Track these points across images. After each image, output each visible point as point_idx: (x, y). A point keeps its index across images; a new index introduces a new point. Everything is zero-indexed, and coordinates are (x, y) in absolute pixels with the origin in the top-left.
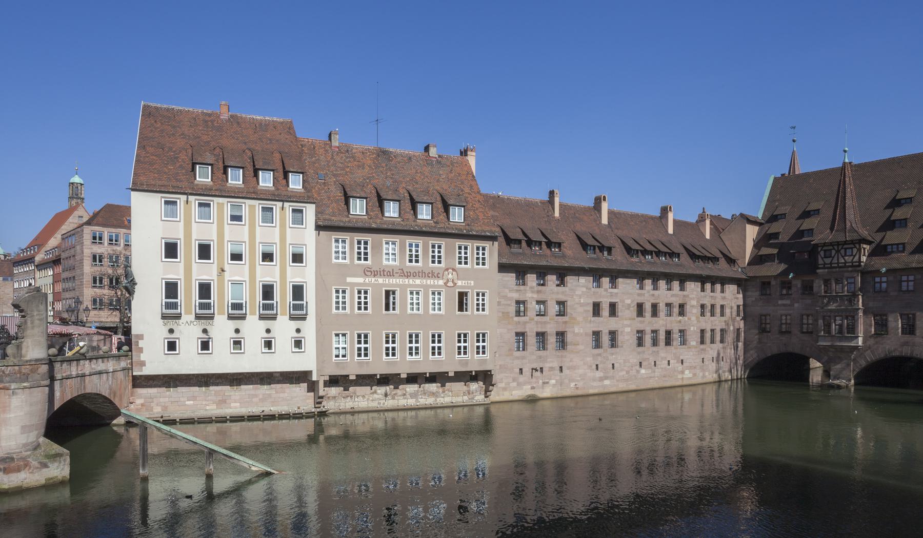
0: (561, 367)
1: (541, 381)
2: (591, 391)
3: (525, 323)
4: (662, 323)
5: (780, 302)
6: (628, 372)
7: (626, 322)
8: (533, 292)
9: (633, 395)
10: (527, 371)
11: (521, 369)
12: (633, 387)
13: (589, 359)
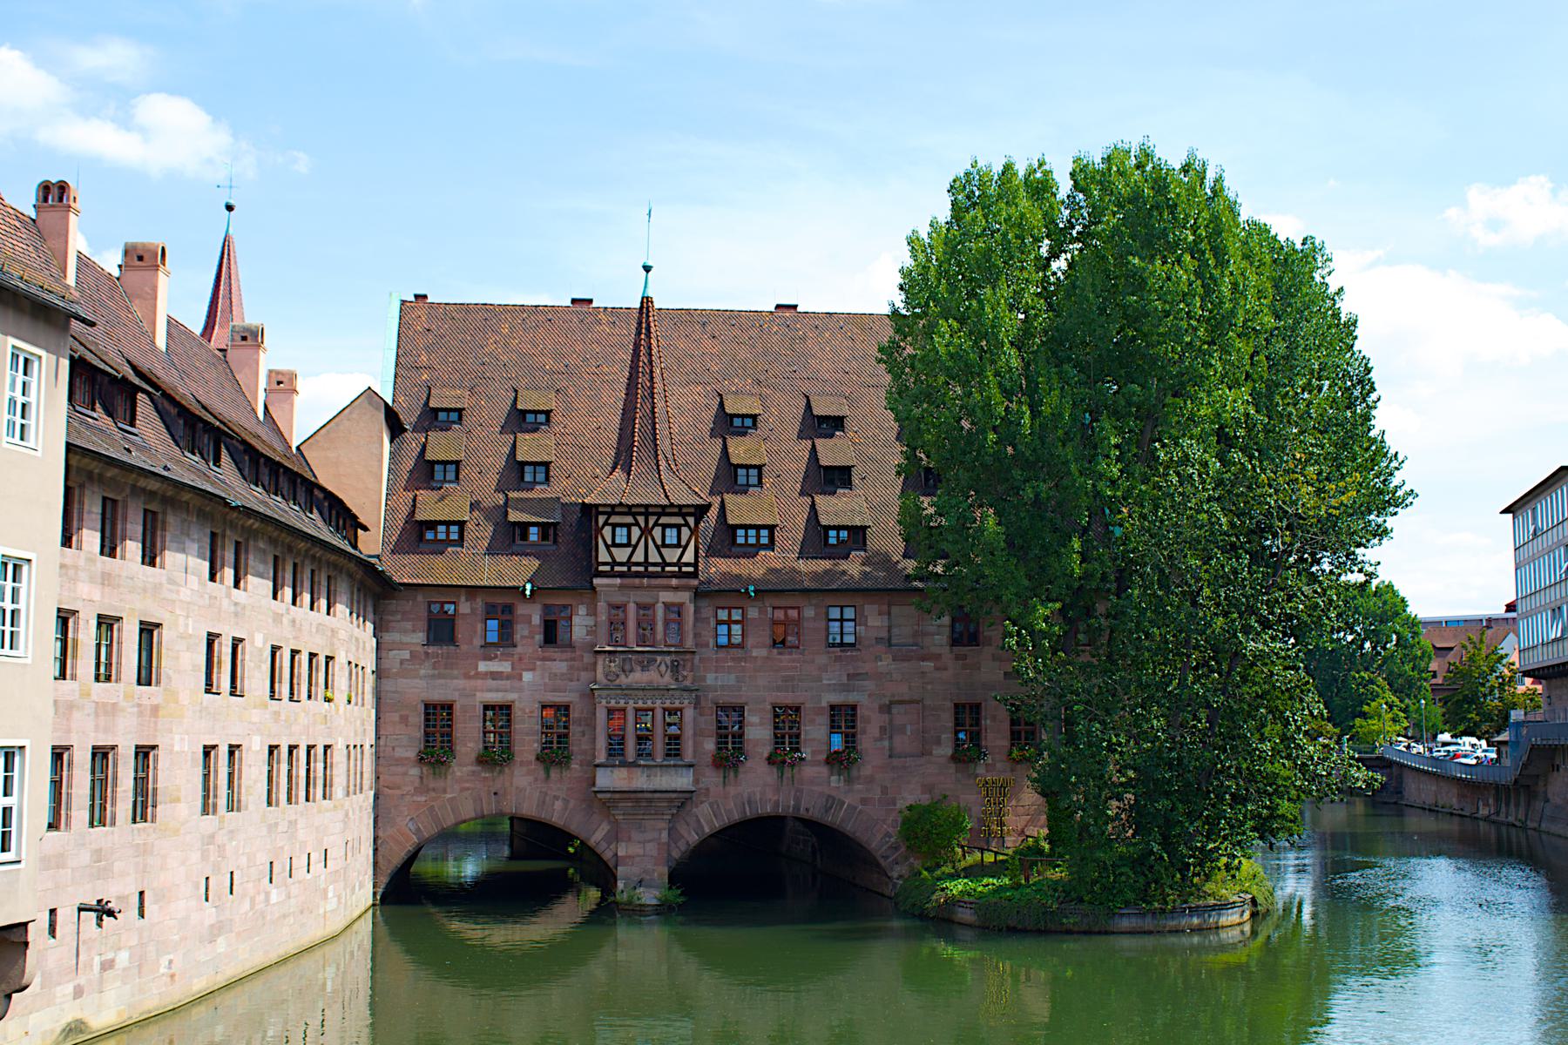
0: (142, 893)
1: (97, 960)
2: (199, 985)
3: (71, 706)
4: (302, 722)
5: (483, 666)
6: (253, 900)
7: (256, 715)
8: (92, 580)
9: (257, 985)
10: (66, 916)
11: (53, 912)
12: (260, 960)
13: (195, 856)
